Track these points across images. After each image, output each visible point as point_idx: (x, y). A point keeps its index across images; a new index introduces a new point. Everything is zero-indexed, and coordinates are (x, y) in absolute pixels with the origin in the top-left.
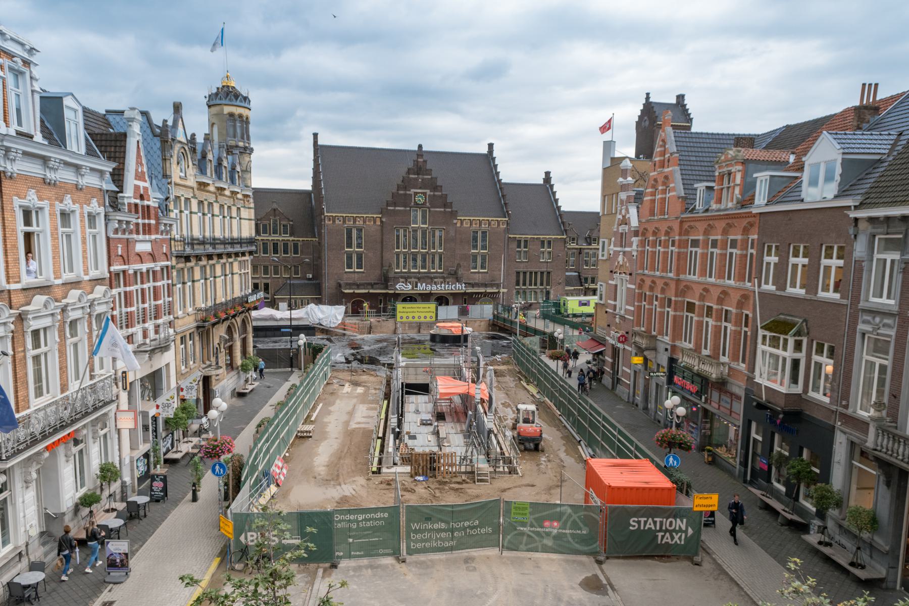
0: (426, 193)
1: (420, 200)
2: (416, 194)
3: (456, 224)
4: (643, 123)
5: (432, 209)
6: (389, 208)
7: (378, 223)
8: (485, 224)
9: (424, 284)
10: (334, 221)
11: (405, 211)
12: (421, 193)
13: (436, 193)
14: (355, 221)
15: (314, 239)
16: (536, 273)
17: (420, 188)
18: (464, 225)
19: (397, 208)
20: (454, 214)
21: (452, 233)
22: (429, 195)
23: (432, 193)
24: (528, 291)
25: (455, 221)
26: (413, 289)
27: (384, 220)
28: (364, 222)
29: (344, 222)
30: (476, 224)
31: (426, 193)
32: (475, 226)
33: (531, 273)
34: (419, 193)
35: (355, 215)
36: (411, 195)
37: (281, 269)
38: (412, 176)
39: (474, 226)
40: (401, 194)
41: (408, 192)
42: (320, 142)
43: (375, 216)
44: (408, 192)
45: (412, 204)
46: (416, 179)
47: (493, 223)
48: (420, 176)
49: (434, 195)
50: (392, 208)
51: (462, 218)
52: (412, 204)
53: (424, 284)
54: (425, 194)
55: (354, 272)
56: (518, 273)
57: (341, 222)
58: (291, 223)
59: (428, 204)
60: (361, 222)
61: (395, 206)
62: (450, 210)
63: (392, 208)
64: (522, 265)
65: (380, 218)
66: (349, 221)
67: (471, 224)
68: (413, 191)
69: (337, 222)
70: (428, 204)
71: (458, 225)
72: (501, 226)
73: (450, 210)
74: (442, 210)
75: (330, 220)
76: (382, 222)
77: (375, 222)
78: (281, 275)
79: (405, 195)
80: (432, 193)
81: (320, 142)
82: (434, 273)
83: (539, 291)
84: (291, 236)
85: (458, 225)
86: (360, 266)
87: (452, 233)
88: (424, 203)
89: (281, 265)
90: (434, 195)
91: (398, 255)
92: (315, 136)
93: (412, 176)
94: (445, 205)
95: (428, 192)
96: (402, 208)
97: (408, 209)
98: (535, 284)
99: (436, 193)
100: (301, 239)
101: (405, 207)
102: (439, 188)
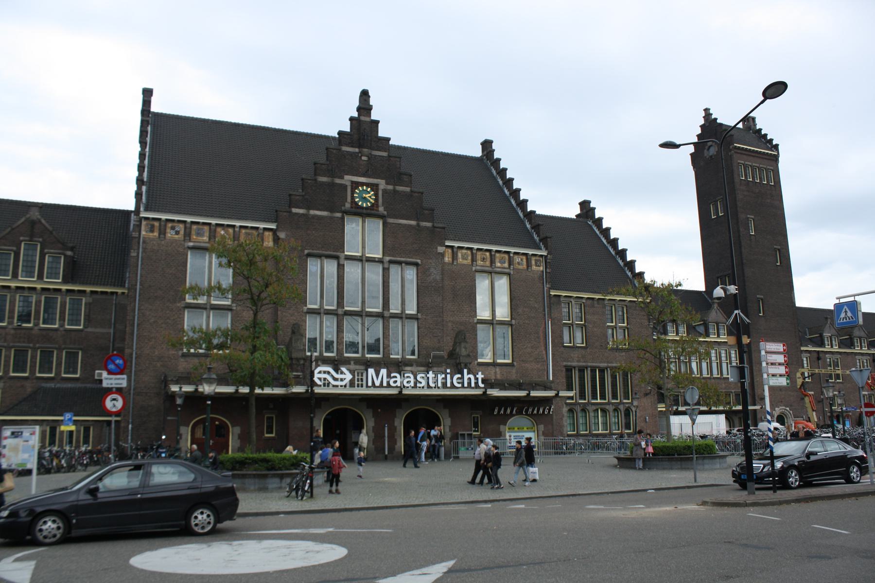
0: (377, 185)
1: (366, 197)
2: (356, 185)
3: (442, 255)
5: (390, 220)
6: (294, 210)
9: (384, 372)
10: (162, 232)
11: (331, 218)
12: (368, 185)
13: (400, 188)
15: (120, 291)
16: (602, 371)
18: (460, 260)
19: (312, 212)
20: (438, 235)
21: (435, 274)
23: (390, 187)
24: (591, 408)
25: (441, 249)
26: (352, 384)
27: (282, 235)
30: (483, 259)
31: (377, 185)
33: (593, 371)
34: (362, 184)
35: (214, 222)
37: (34, 357)
38: (345, 149)
39: (480, 262)
40: (323, 183)
41: (338, 181)
42: (155, 108)
43: (262, 225)
44: (338, 181)
45: (348, 205)
47: (517, 259)
49: (395, 191)
50: (301, 211)
51: (456, 244)
52: (348, 205)
53: (384, 372)
54: (374, 187)
56: (569, 370)
58: (69, 253)
59: (381, 209)
61: (309, 208)
62: (429, 224)
63: (301, 211)
64: (575, 354)
66: (198, 234)
67: (474, 260)
68: (349, 179)
69: (170, 234)
70: (381, 209)
71: (447, 259)
72: (534, 268)
73: (429, 224)
74: (413, 223)
75: (152, 230)
78: (33, 372)
79: (332, 185)
80: (390, 187)
81: (155, 108)
83: (611, 408)
84: (65, 281)
85: (447, 259)
87: (435, 274)
88: (375, 205)
89: (35, 349)
90: (395, 191)
92: (148, 94)
93: (345, 149)
95: (382, 184)
96: (325, 213)
97: (339, 215)
98: (603, 397)
99: (400, 188)
100: (88, 289)
102: (406, 178)
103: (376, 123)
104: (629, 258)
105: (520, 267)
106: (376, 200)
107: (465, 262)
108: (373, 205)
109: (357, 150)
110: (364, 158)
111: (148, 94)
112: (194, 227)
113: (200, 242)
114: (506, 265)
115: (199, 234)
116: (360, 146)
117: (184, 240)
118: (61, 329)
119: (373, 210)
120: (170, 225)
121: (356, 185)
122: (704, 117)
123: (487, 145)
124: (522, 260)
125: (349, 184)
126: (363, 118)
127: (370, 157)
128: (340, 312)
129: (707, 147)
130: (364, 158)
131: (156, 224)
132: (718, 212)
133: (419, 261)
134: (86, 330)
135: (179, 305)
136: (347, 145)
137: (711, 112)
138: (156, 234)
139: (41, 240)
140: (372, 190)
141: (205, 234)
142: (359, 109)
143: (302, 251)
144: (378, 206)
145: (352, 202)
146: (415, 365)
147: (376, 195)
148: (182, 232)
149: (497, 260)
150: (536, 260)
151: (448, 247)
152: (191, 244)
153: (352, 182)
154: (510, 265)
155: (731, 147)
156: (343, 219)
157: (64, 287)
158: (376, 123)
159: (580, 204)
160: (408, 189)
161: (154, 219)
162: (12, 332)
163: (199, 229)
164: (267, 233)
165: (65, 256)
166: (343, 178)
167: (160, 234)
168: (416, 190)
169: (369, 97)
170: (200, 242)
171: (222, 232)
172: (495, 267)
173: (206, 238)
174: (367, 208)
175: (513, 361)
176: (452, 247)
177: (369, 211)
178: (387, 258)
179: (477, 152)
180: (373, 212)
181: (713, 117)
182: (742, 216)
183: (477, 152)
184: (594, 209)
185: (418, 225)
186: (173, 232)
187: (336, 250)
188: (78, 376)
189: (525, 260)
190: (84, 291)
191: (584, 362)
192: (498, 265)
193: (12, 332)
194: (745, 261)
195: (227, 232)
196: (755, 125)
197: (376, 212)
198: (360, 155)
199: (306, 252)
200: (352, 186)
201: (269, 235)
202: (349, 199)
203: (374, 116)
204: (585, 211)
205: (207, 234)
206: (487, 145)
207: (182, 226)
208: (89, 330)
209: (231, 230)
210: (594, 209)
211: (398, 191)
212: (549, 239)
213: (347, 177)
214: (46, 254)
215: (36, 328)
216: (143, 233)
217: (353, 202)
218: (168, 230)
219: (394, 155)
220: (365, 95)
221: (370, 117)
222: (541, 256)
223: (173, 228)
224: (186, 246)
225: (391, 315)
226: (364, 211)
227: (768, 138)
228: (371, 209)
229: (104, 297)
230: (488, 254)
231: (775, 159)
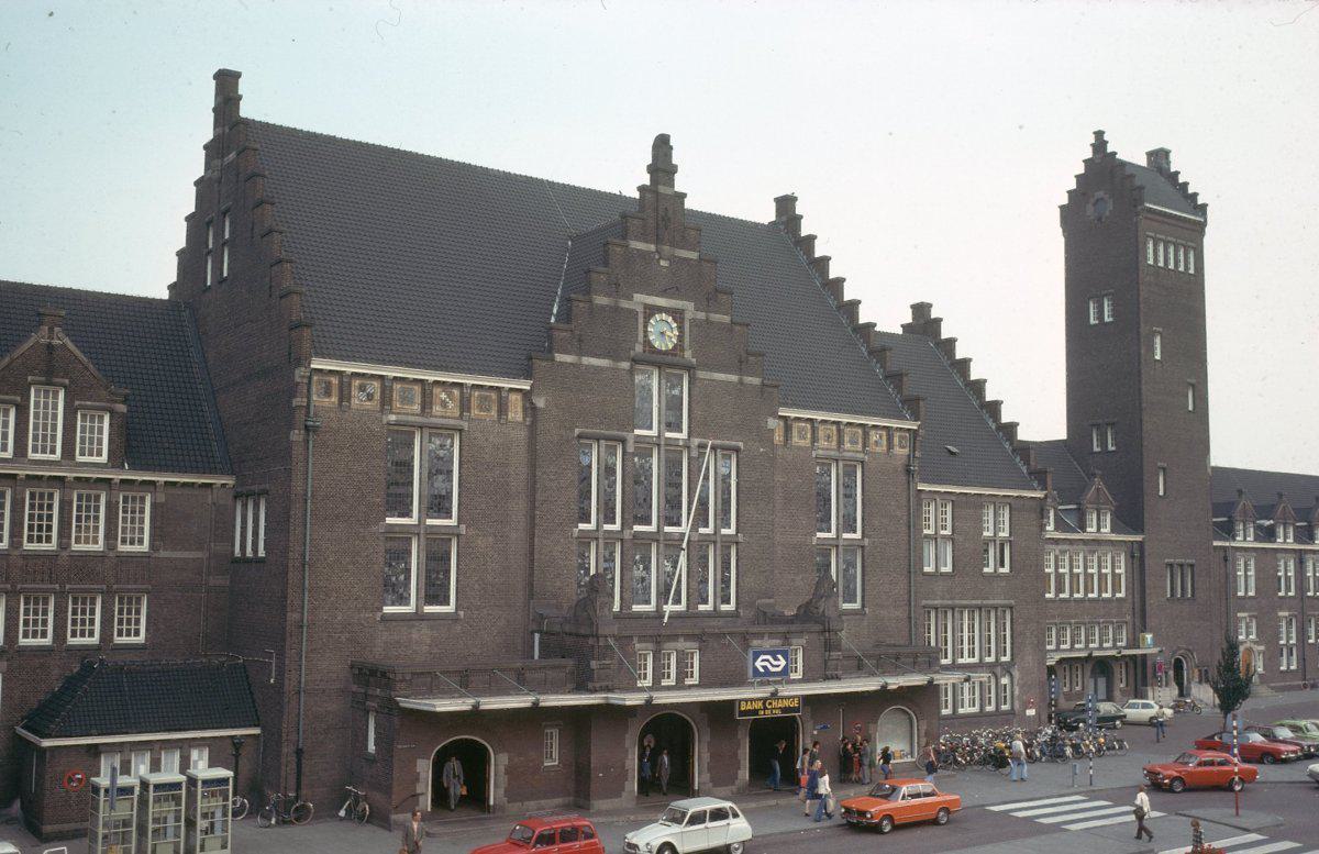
1: (662, 333)
4: (1090, 210)
5: (701, 374)
6: (559, 357)
7: (516, 413)
8: (853, 442)
10: (345, 396)
13: (716, 317)
14: (426, 404)
17: (663, 293)
18: (795, 439)
19: (587, 360)
22: (693, 322)
23: (701, 315)
25: (772, 423)
27: (540, 403)
28: (465, 406)
29: (386, 400)
32: (825, 446)
34: (660, 310)
36: (633, 314)
39: (823, 443)
40: (603, 308)
42: (247, 110)
43: (506, 384)
44: (624, 304)
45: (639, 348)
46: (643, 254)
47: (874, 436)
48: (666, 248)
50: (568, 359)
51: (792, 413)
52: (639, 348)
54: (677, 315)
55: (419, 617)
57: (374, 405)
58: (122, 408)
59: (688, 354)
60: (453, 408)
61: (581, 353)
62: (756, 381)
63: (568, 359)
65: (526, 394)
68: (641, 298)
69: (358, 400)
70: (688, 354)
71: (778, 438)
74: (734, 378)
75: (328, 393)
76: (530, 409)
77: (503, 409)
79: (616, 309)
80: (701, 315)
81: (247, 110)
82: (707, 615)
86: (435, 593)
88: (679, 347)
91: (585, 540)
92: (227, 82)
94: (741, 366)
95: (688, 306)
97: (625, 365)
99: (716, 317)
100: (161, 478)
101: (616, 357)
103: (683, 196)
104: (1005, 418)
105: (878, 449)
106: (680, 338)
107: (802, 443)
108: (675, 347)
109: (652, 247)
110: (662, 263)
111: (227, 82)
112: (397, 386)
113: (408, 414)
114: (860, 447)
115: (406, 400)
116: (658, 241)
117: (382, 411)
118: (111, 554)
119: (676, 355)
120: (357, 383)
121: (651, 311)
122: (1092, 145)
123: (785, 204)
124: (881, 437)
125: (640, 309)
126: (662, 189)
127: (672, 259)
128: (627, 535)
129: (1092, 200)
130: (662, 263)
131: (335, 380)
132: (1103, 312)
133: (741, 444)
134: (157, 555)
135: (374, 529)
136: (637, 239)
137: (1106, 138)
138: (334, 399)
139: (67, 381)
140: (675, 320)
141: (416, 400)
142: (652, 169)
143: (572, 430)
144: (683, 350)
145: (645, 341)
146: (766, 638)
147: (680, 328)
148: (377, 396)
149: (847, 439)
150: (900, 437)
151: (781, 417)
152: (393, 418)
153: (646, 306)
154: (864, 445)
155: (1139, 208)
156: (631, 372)
157: (117, 476)
158: (683, 196)
159: (913, 307)
160: (726, 319)
161: (331, 372)
162: (21, 562)
163: (404, 391)
164: (513, 397)
165: (112, 413)
166: (630, 298)
167: (341, 400)
168: (739, 320)
169: (671, 148)
170: (408, 414)
171: (443, 396)
172: (844, 451)
173: (417, 408)
174: (666, 353)
175: (863, 606)
176: (785, 418)
177: (669, 359)
178: (696, 441)
179: (766, 214)
180: (676, 360)
181: (1109, 150)
182: (1144, 329)
183: (766, 214)
184: (938, 321)
185: (741, 382)
186: (363, 396)
187: (623, 427)
188: (141, 639)
189: (885, 438)
190: (153, 483)
191: (951, 599)
192: (847, 446)
193: (21, 562)
194: (1144, 405)
195: (450, 395)
196: (1168, 163)
197: (681, 361)
198: (657, 257)
199: (577, 431)
200: (645, 312)
201: (517, 400)
202: (641, 338)
203: (679, 186)
204: (922, 321)
205: (418, 399)
206: (785, 204)
207: (376, 384)
208: (163, 554)
209: (456, 392)
210: (938, 321)
211: (712, 323)
212: (921, 403)
213: (638, 297)
214: (30, 384)
215: (64, 554)
216: (315, 398)
217: (647, 343)
218: (355, 392)
219: (707, 258)
220: (662, 145)
221: (674, 187)
222: (909, 430)
223: (362, 388)
224: (385, 421)
225: (701, 538)
226: (659, 358)
227: (1199, 203)
228: (672, 355)
229: (187, 491)
230: (834, 428)
231: (1200, 228)
